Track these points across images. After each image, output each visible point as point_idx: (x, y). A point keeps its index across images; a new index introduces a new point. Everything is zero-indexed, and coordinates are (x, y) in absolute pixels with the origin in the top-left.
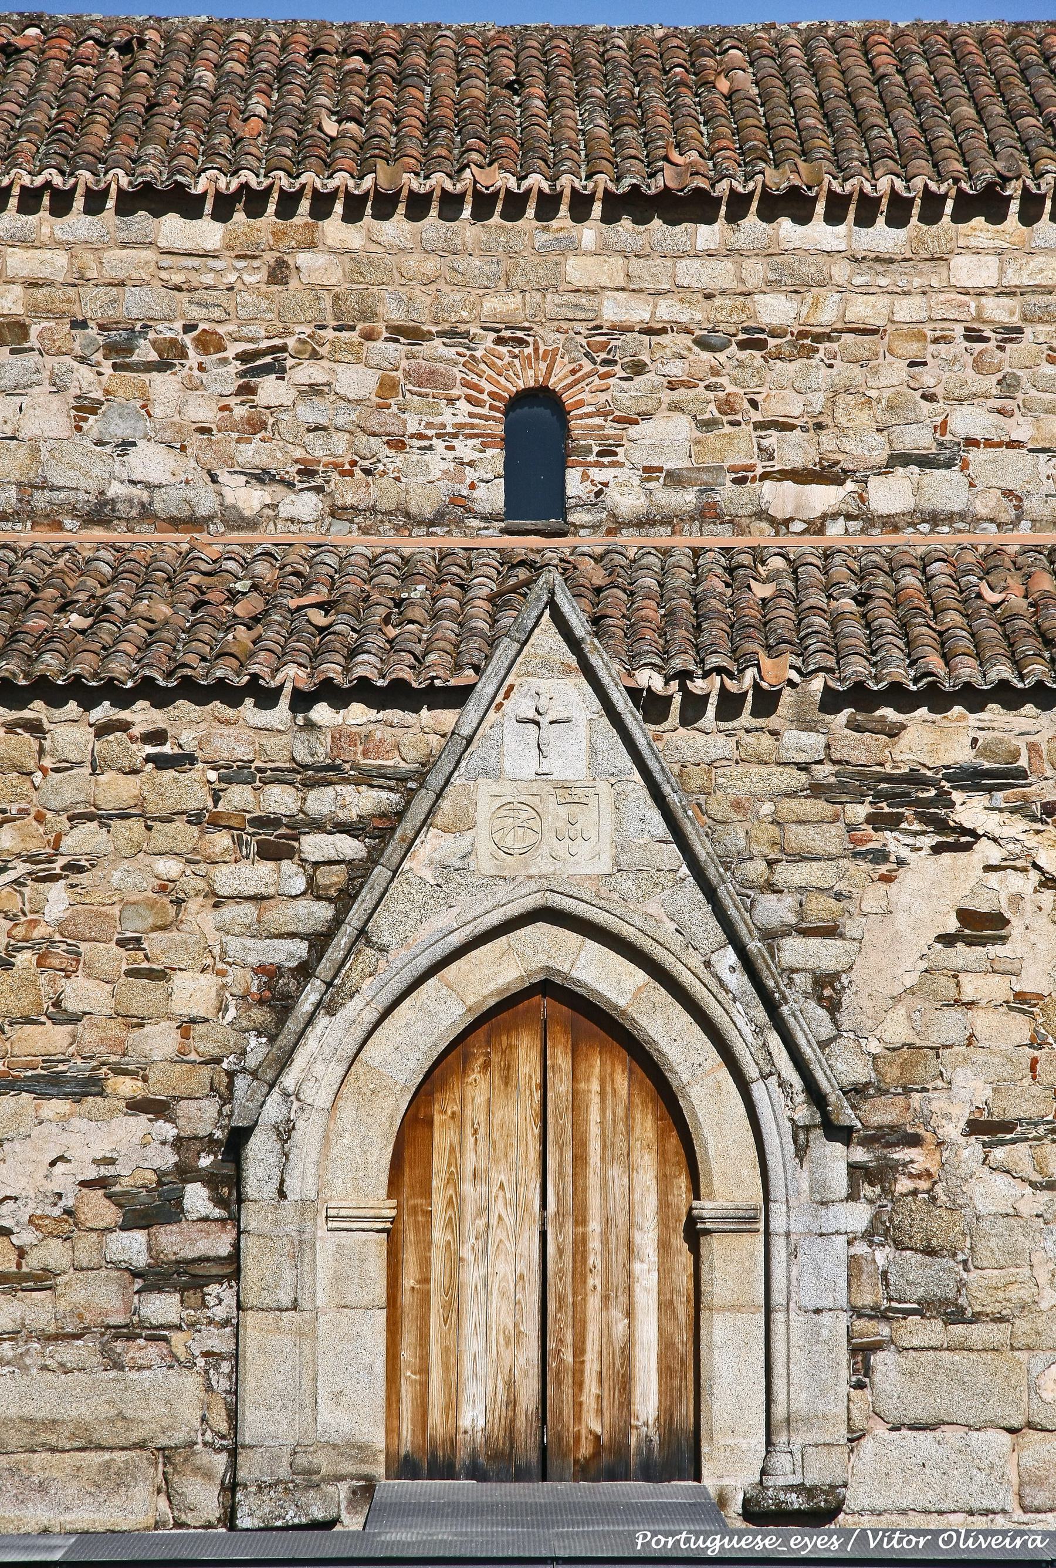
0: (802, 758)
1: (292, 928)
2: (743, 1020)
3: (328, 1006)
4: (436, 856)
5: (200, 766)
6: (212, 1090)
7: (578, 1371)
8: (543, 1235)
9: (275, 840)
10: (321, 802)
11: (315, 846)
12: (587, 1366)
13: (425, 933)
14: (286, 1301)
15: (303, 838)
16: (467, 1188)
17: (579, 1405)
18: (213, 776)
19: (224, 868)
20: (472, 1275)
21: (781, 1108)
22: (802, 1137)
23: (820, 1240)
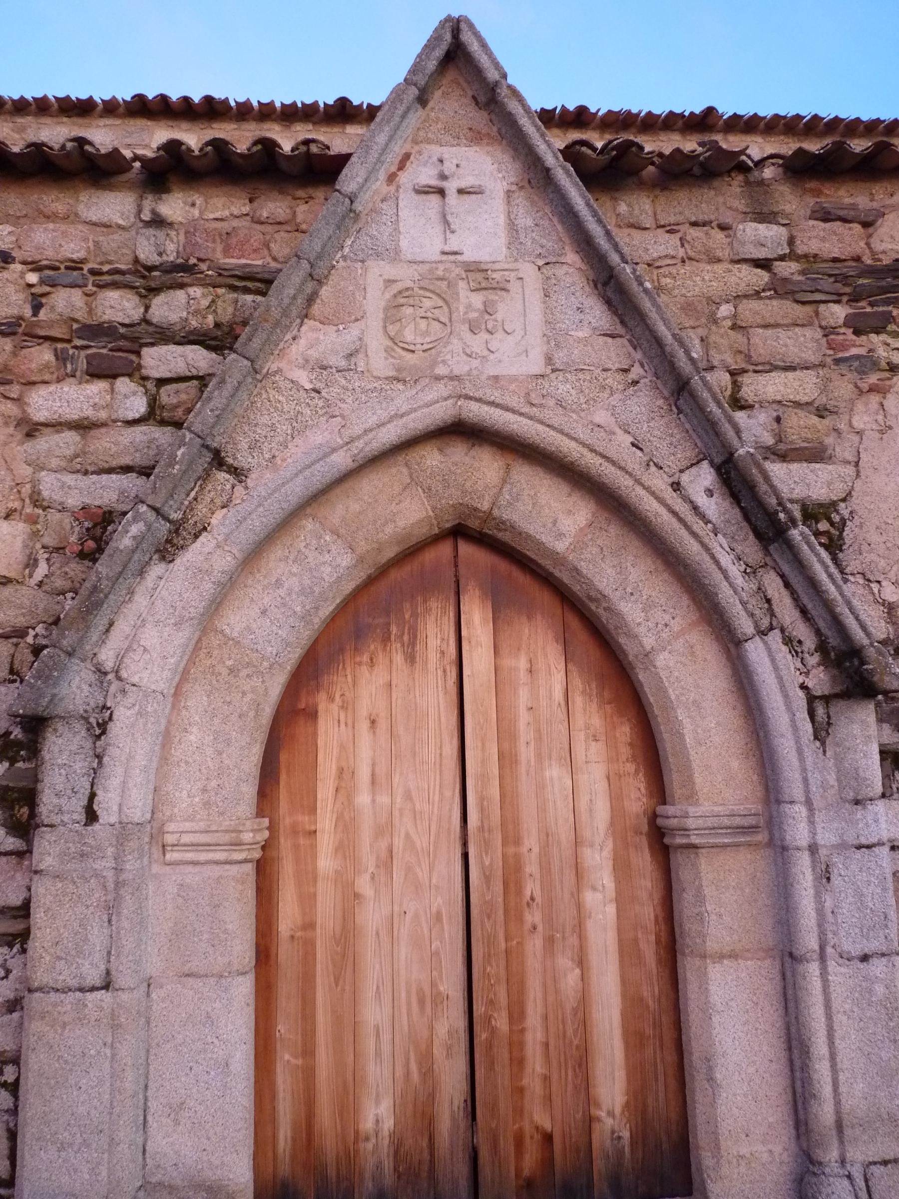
0: (761, 254)
1: (126, 460)
2: (726, 558)
3: (167, 550)
4: (313, 353)
5: (17, 267)
6: (12, 671)
7: (516, 1044)
8: (465, 856)
9: (111, 352)
10: (170, 308)
11: (160, 360)
12: (529, 1037)
13: (297, 452)
14: (94, 977)
15: (145, 351)
16: (363, 799)
17: (519, 1091)
18: (32, 278)
19: (43, 391)
20: (371, 917)
21: (782, 674)
22: (820, 711)
23: (858, 854)
